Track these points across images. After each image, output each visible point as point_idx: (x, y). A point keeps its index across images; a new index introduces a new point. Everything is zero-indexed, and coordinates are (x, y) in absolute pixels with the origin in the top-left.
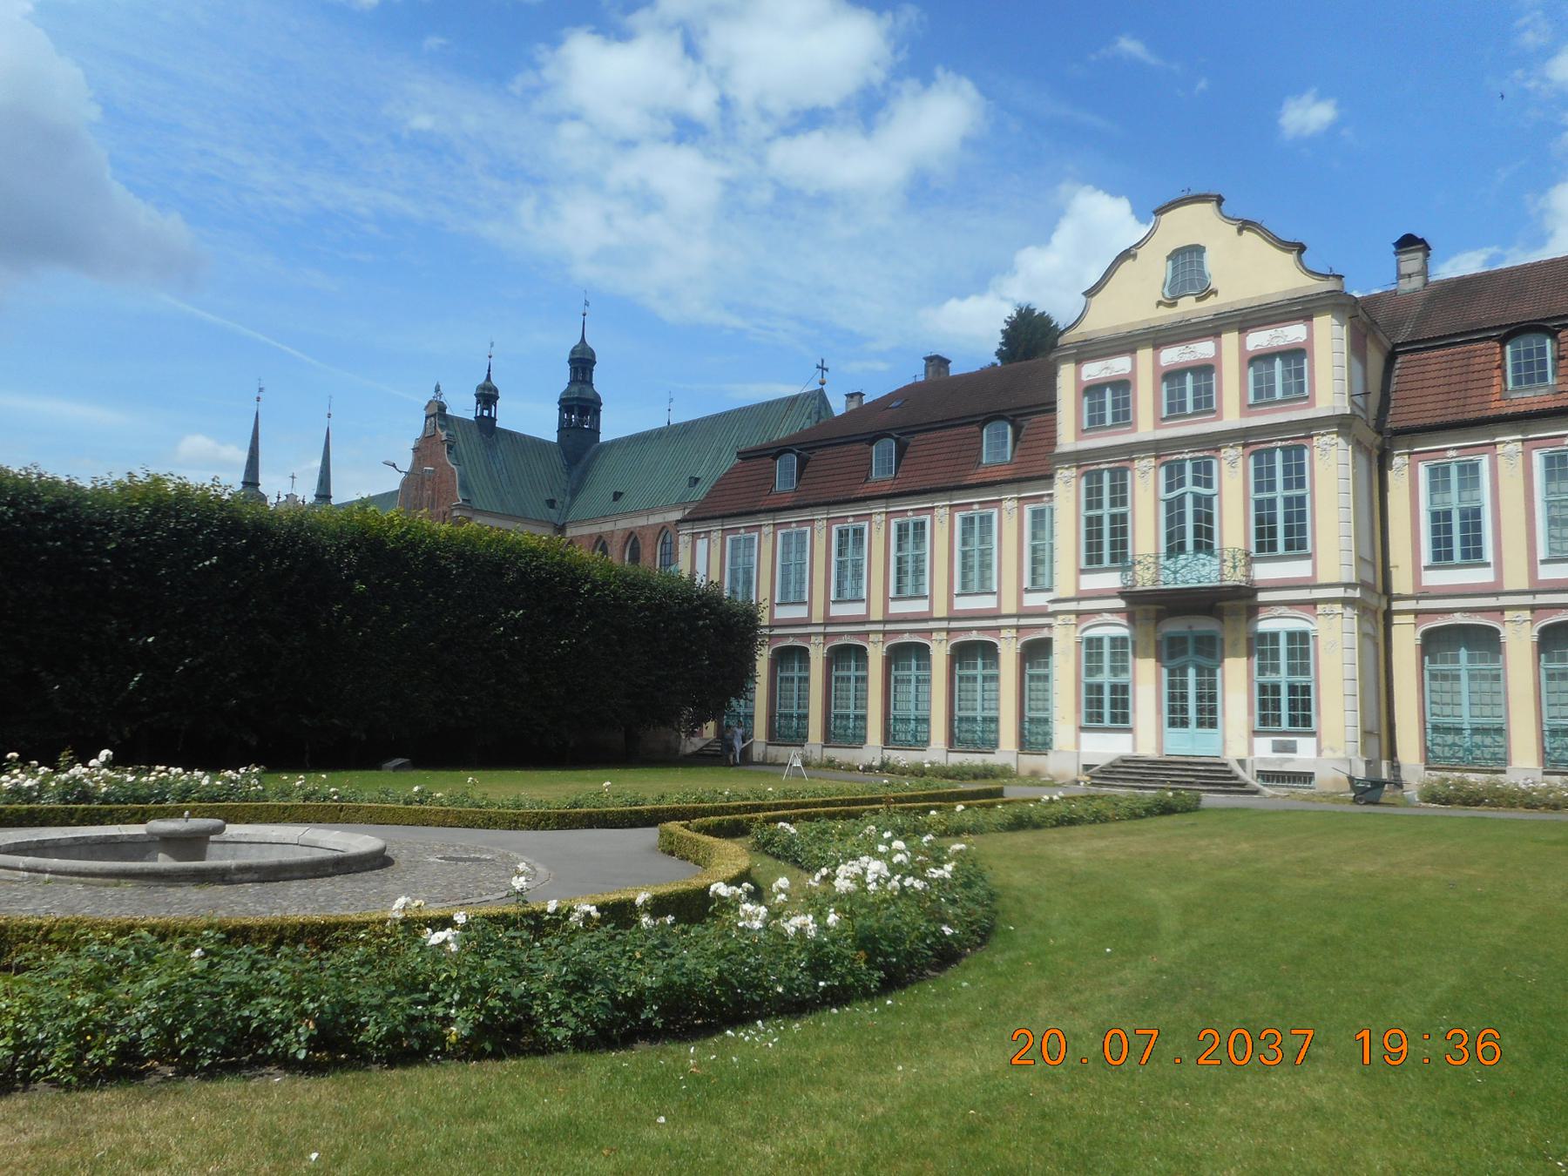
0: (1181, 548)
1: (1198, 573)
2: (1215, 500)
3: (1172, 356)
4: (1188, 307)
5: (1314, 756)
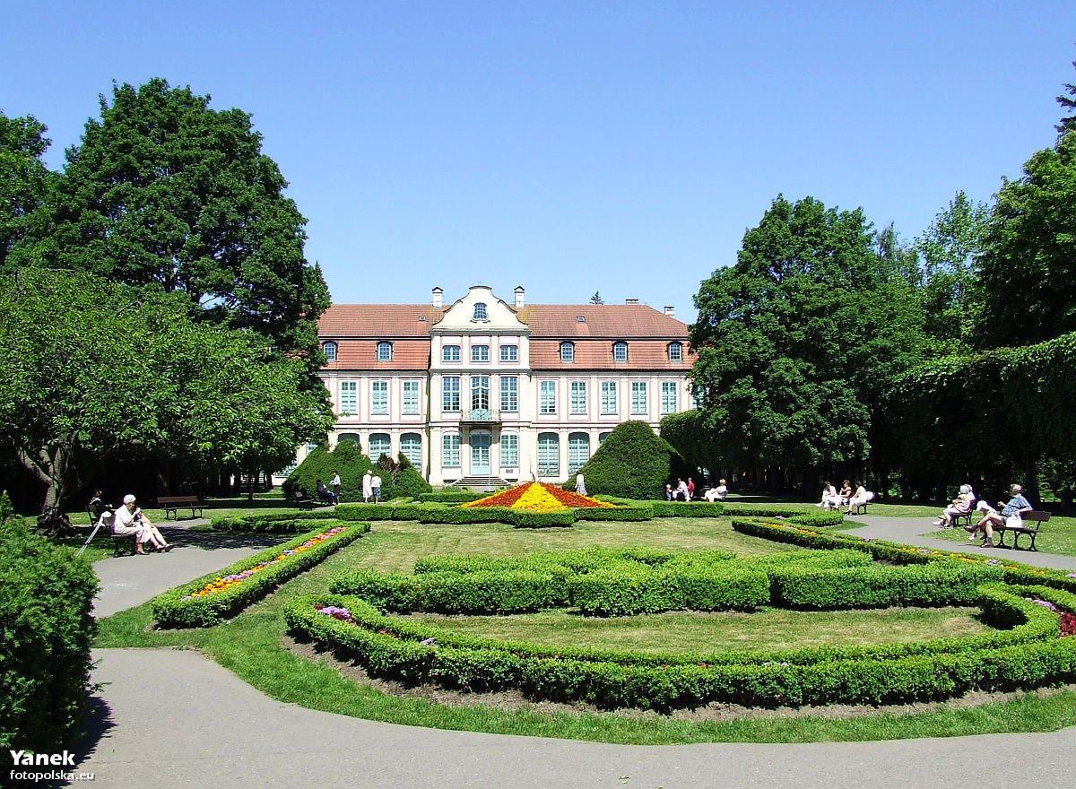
0: (478, 407)
2: (489, 392)
3: (477, 340)
4: (480, 325)
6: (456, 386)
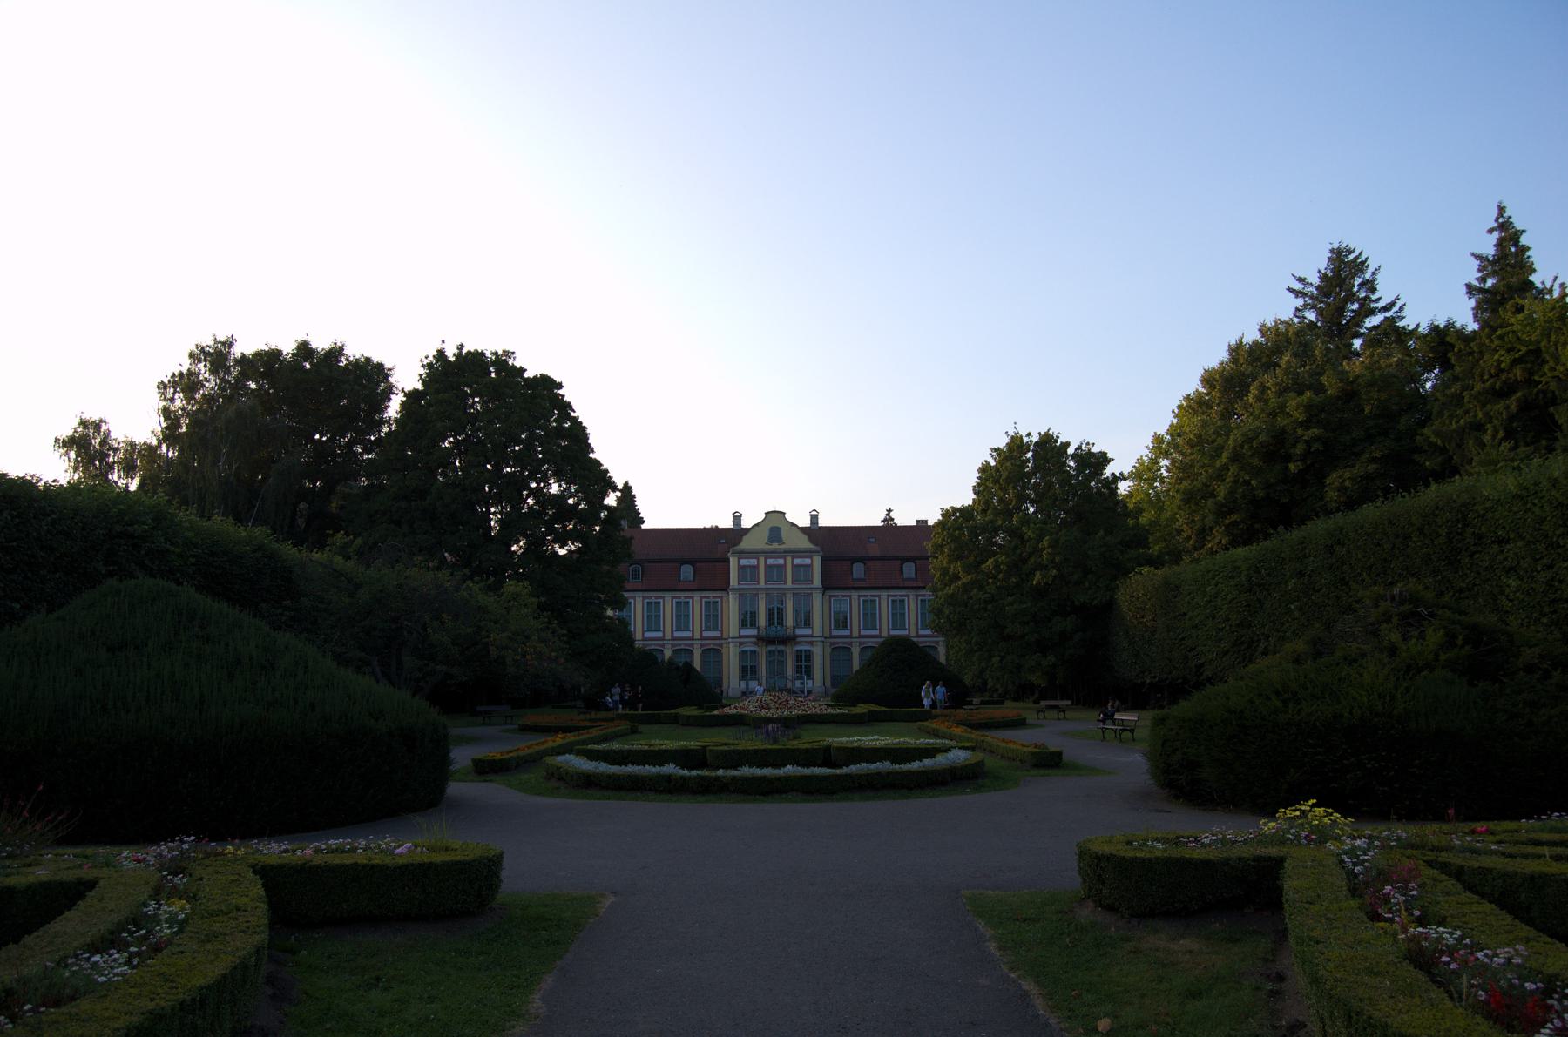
4: (775, 546)
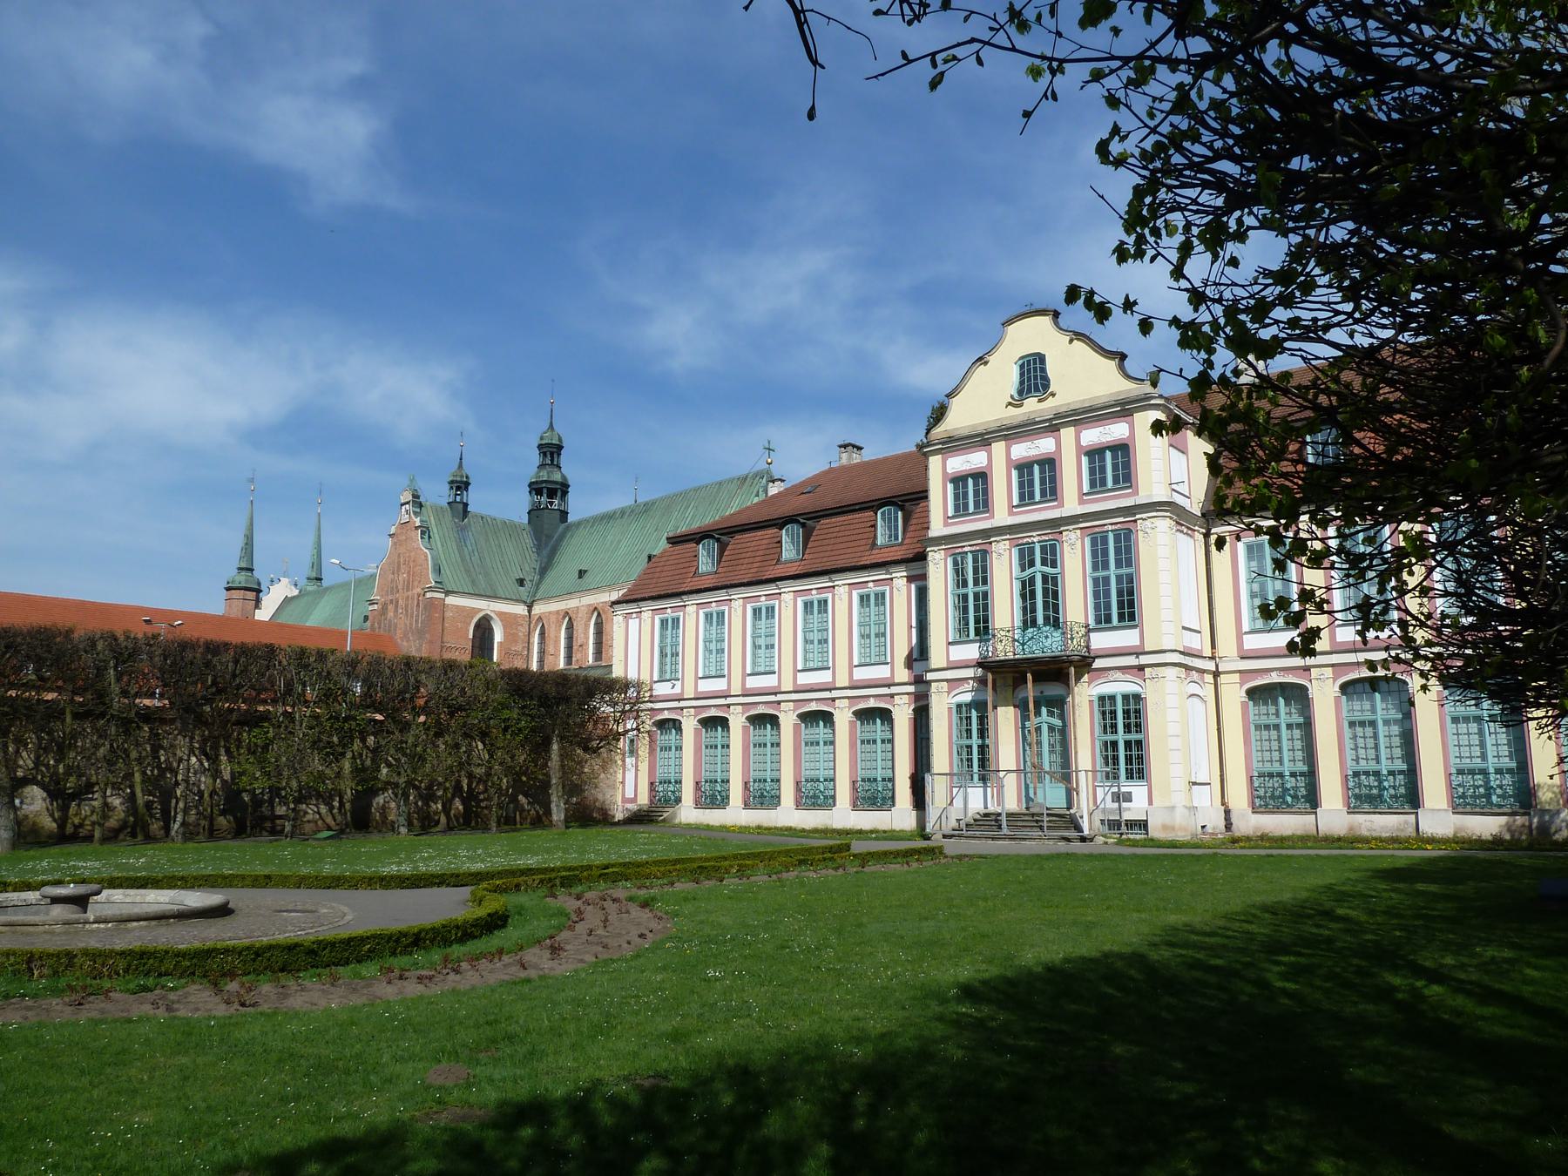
0: (1034, 623)
1: (1049, 644)
5: (1146, 805)
6: (982, 576)
